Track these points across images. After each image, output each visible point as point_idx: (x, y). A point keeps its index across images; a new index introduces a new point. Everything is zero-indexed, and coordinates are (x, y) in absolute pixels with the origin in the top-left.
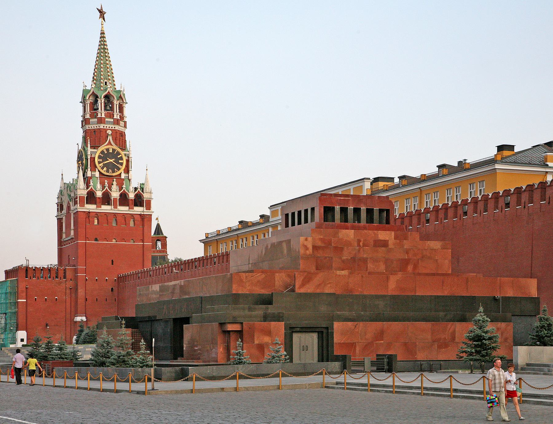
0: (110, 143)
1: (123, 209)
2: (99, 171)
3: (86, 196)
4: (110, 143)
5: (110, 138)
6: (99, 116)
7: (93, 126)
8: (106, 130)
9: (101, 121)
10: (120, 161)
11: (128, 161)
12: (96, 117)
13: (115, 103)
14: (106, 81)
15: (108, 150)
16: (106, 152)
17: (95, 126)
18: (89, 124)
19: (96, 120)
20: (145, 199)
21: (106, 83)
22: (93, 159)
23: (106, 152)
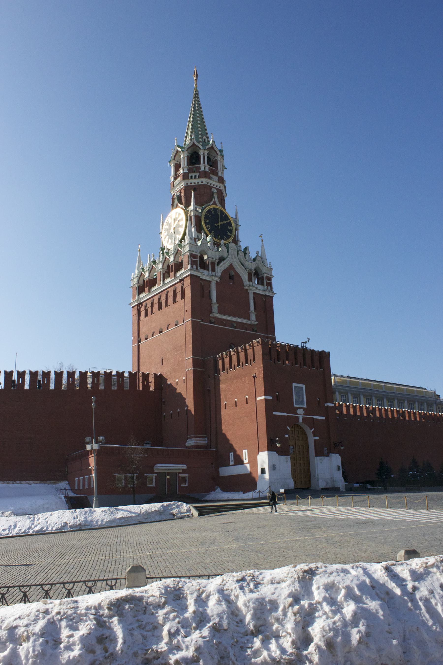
0: (215, 204)
2: (205, 233)
3: (199, 255)
4: (215, 204)
5: (216, 197)
6: (202, 169)
7: (192, 181)
8: (210, 188)
9: (205, 175)
10: (229, 228)
11: (236, 229)
12: (195, 172)
13: (219, 159)
14: (205, 137)
15: (215, 210)
18: (188, 178)
19: (198, 174)
21: (205, 140)
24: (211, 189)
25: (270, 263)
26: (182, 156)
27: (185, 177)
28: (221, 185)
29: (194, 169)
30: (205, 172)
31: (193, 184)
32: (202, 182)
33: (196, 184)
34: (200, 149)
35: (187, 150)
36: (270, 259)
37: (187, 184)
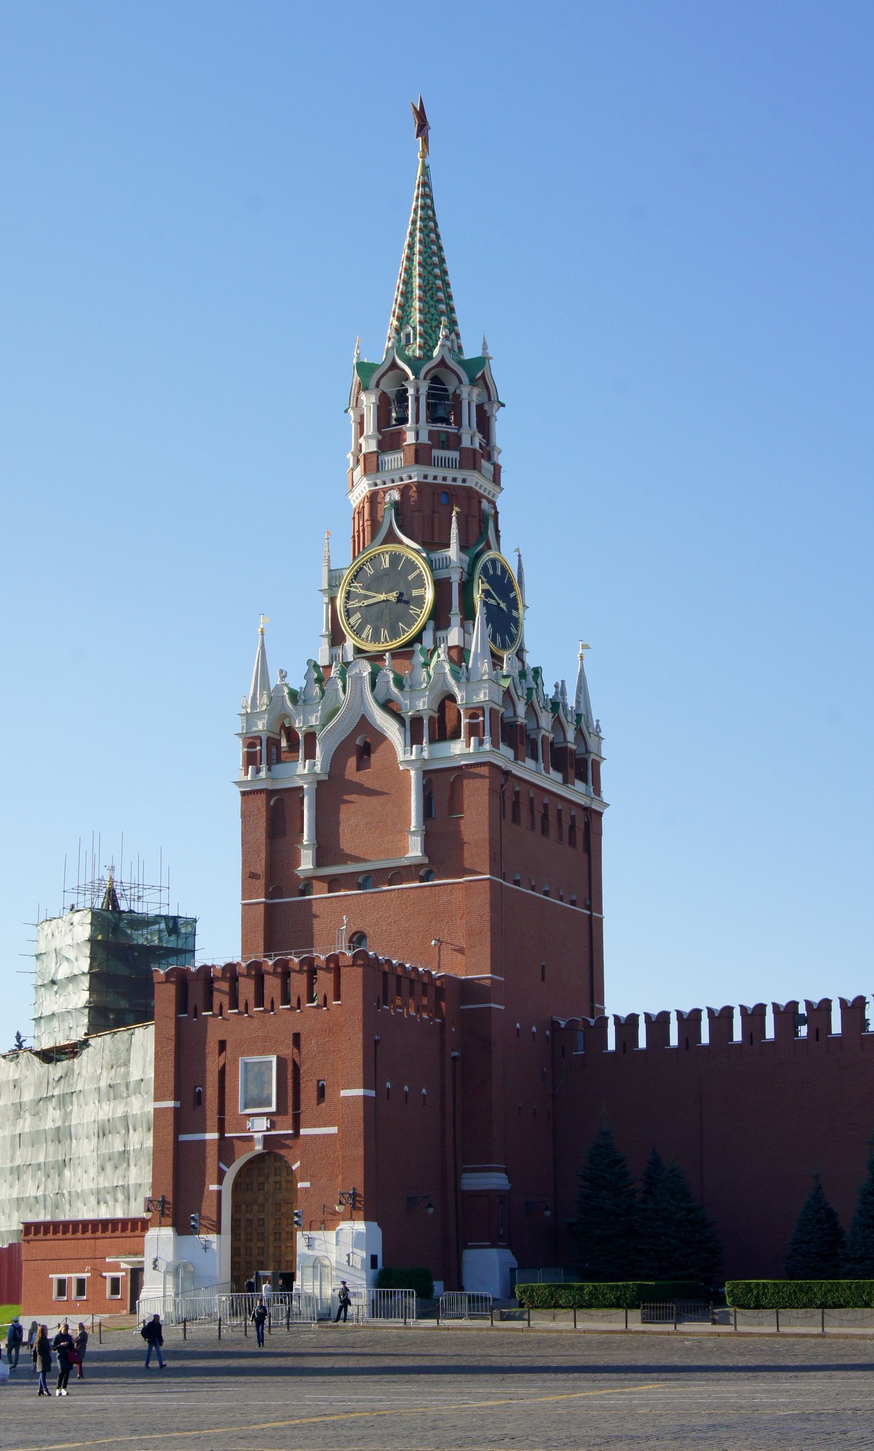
1: (551, 781)
6: (466, 443)
7: (440, 472)
8: (480, 496)
12: (445, 446)
16: (491, 572)
17: (450, 474)
19: (455, 455)
20: (593, 756)
22: (466, 588)
23: (491, 572)
24: (480, 502)
25: (598, 721)
26: (411, 392)
27: (421, 455)
28: (497, 488)
29: (443, 438)
30: (474, 450)
31: (439, 481)
32: (464, 481)
33: (449, 482)
34: (461, 382)
35: (425, 378)
36: (599, 712)
37: (425, 477)
